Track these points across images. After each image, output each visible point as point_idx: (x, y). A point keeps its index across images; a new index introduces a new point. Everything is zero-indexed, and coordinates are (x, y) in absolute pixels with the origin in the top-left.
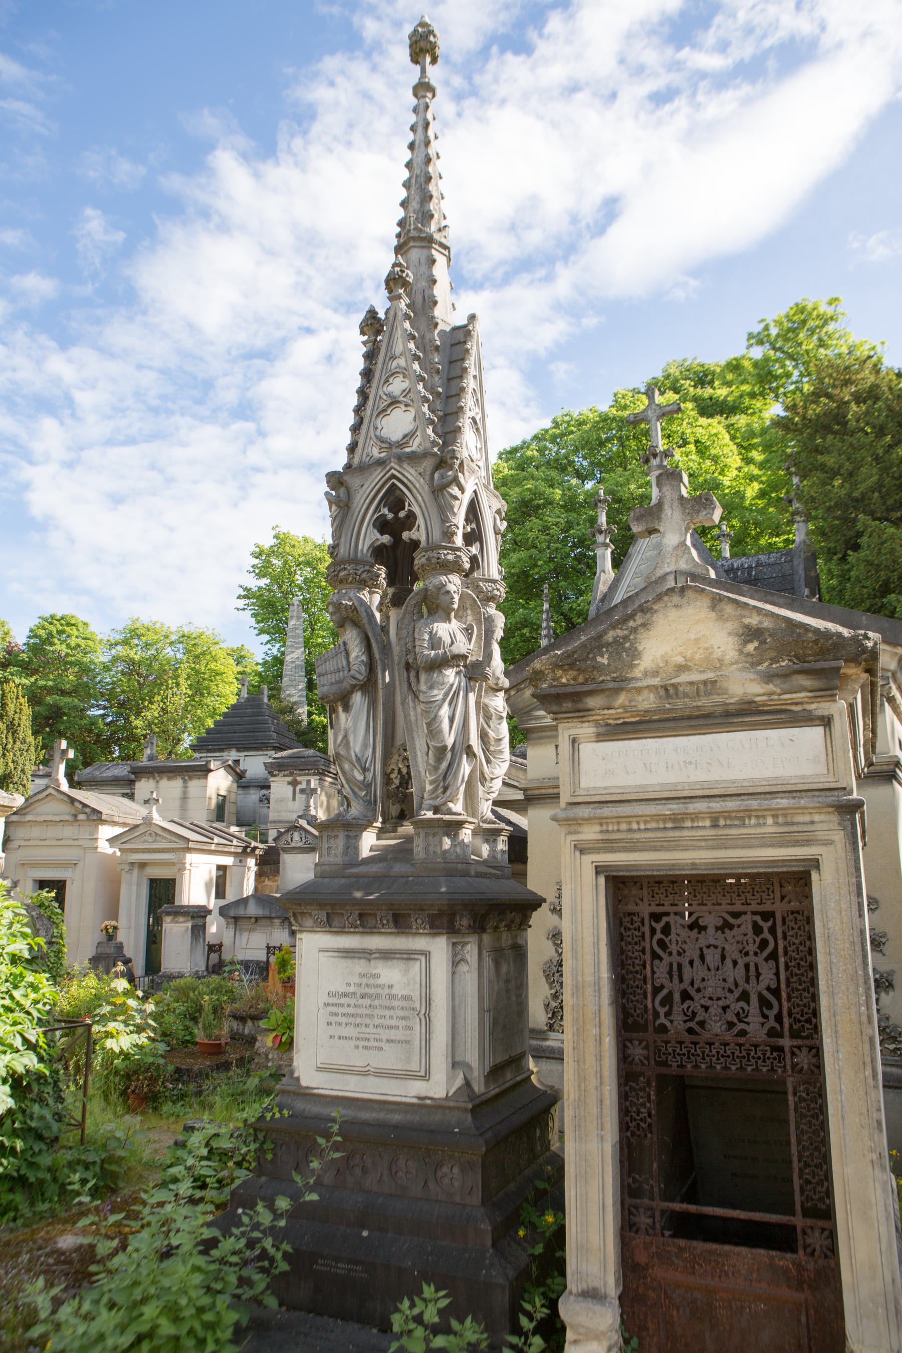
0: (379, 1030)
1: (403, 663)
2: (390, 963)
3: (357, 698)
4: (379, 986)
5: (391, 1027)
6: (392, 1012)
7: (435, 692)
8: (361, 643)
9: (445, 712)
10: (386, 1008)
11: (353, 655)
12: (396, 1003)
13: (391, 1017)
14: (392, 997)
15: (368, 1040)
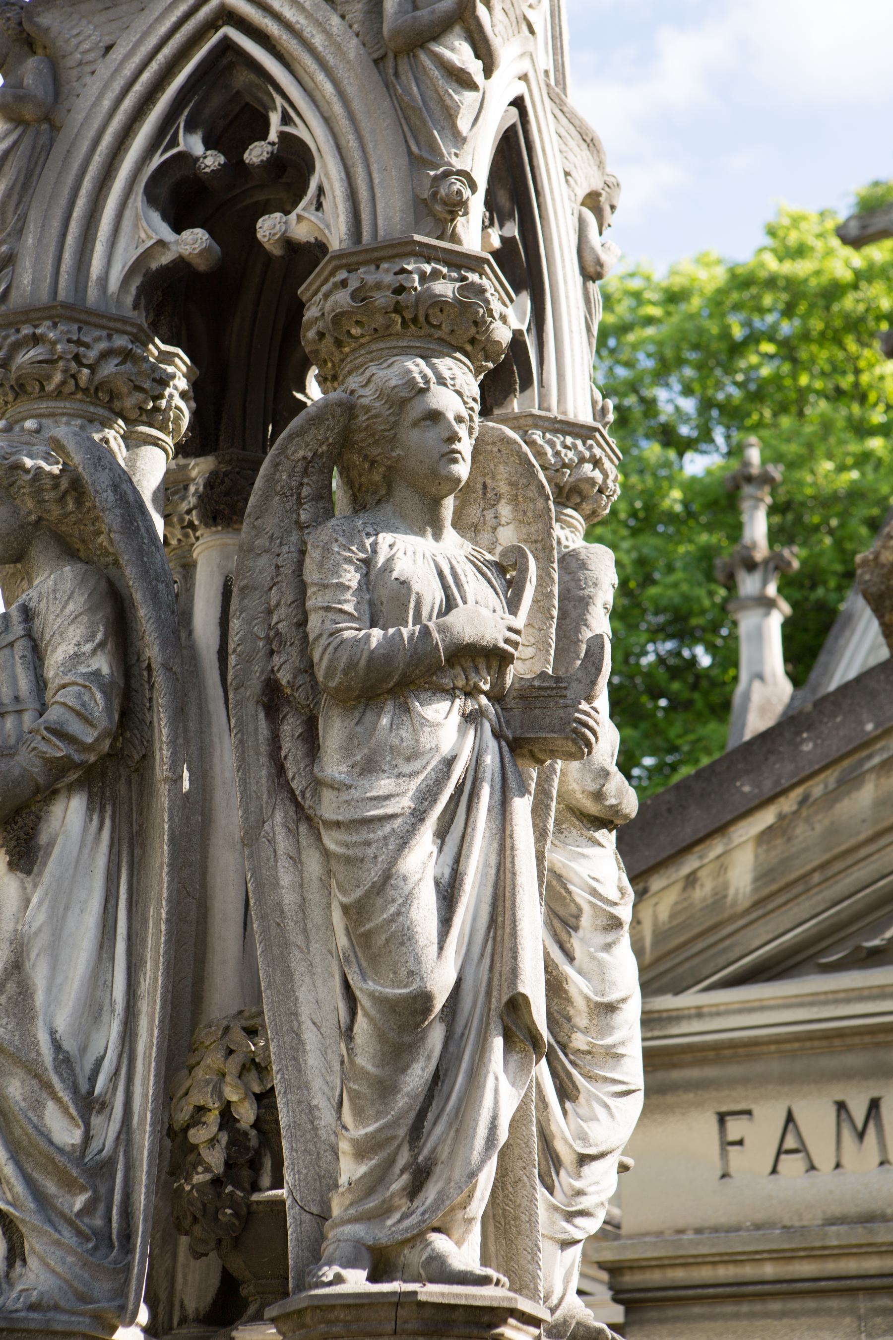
1: (255, 683)
3: (70, 819)
7: (384, 785)
8: (91, 610)
9: (421, 861)
11: (57, 656)
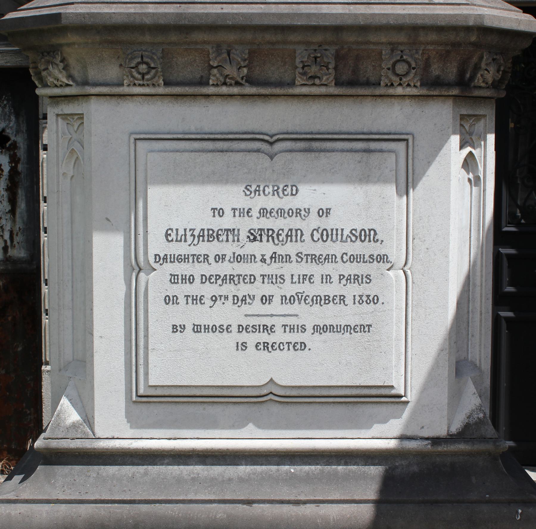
0: (295, 308)
2: (324, 159)
4: (298, 212)
5: (327, 300)
6: (328, 268)
10: (315, 259)
12: (335, 248)
13: (327, 279)
14: (326, 235)
15: (268, 329)
